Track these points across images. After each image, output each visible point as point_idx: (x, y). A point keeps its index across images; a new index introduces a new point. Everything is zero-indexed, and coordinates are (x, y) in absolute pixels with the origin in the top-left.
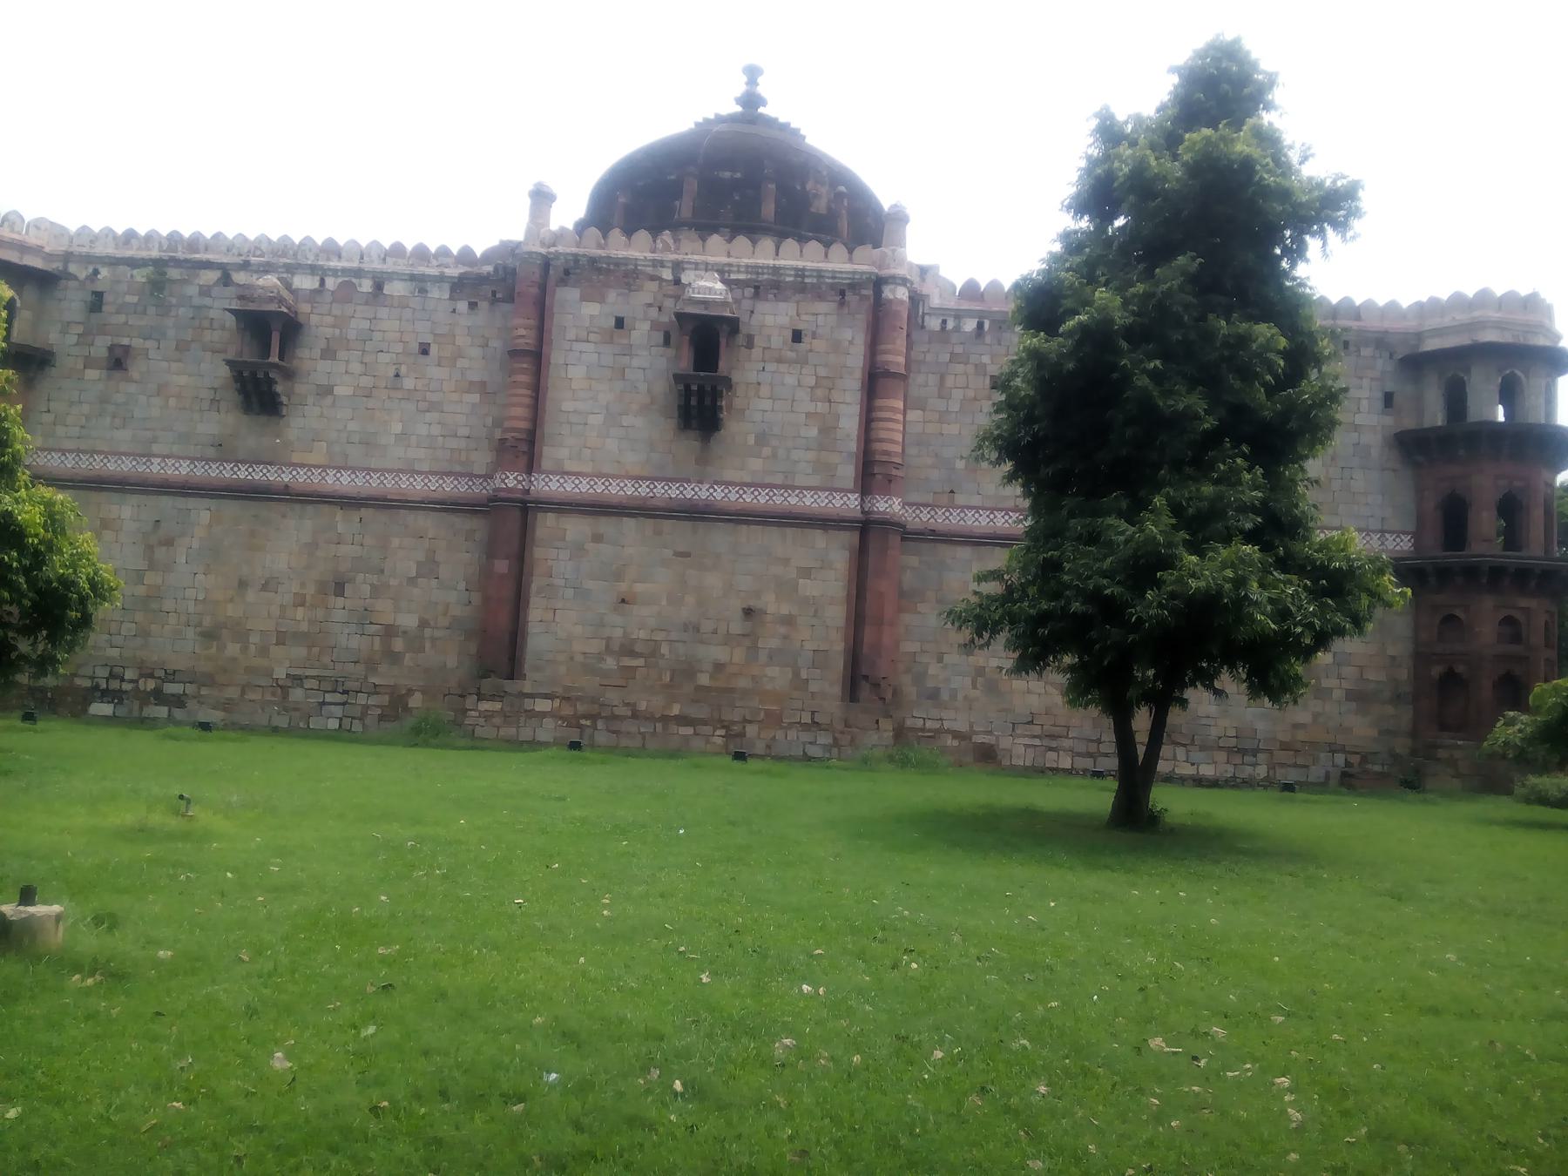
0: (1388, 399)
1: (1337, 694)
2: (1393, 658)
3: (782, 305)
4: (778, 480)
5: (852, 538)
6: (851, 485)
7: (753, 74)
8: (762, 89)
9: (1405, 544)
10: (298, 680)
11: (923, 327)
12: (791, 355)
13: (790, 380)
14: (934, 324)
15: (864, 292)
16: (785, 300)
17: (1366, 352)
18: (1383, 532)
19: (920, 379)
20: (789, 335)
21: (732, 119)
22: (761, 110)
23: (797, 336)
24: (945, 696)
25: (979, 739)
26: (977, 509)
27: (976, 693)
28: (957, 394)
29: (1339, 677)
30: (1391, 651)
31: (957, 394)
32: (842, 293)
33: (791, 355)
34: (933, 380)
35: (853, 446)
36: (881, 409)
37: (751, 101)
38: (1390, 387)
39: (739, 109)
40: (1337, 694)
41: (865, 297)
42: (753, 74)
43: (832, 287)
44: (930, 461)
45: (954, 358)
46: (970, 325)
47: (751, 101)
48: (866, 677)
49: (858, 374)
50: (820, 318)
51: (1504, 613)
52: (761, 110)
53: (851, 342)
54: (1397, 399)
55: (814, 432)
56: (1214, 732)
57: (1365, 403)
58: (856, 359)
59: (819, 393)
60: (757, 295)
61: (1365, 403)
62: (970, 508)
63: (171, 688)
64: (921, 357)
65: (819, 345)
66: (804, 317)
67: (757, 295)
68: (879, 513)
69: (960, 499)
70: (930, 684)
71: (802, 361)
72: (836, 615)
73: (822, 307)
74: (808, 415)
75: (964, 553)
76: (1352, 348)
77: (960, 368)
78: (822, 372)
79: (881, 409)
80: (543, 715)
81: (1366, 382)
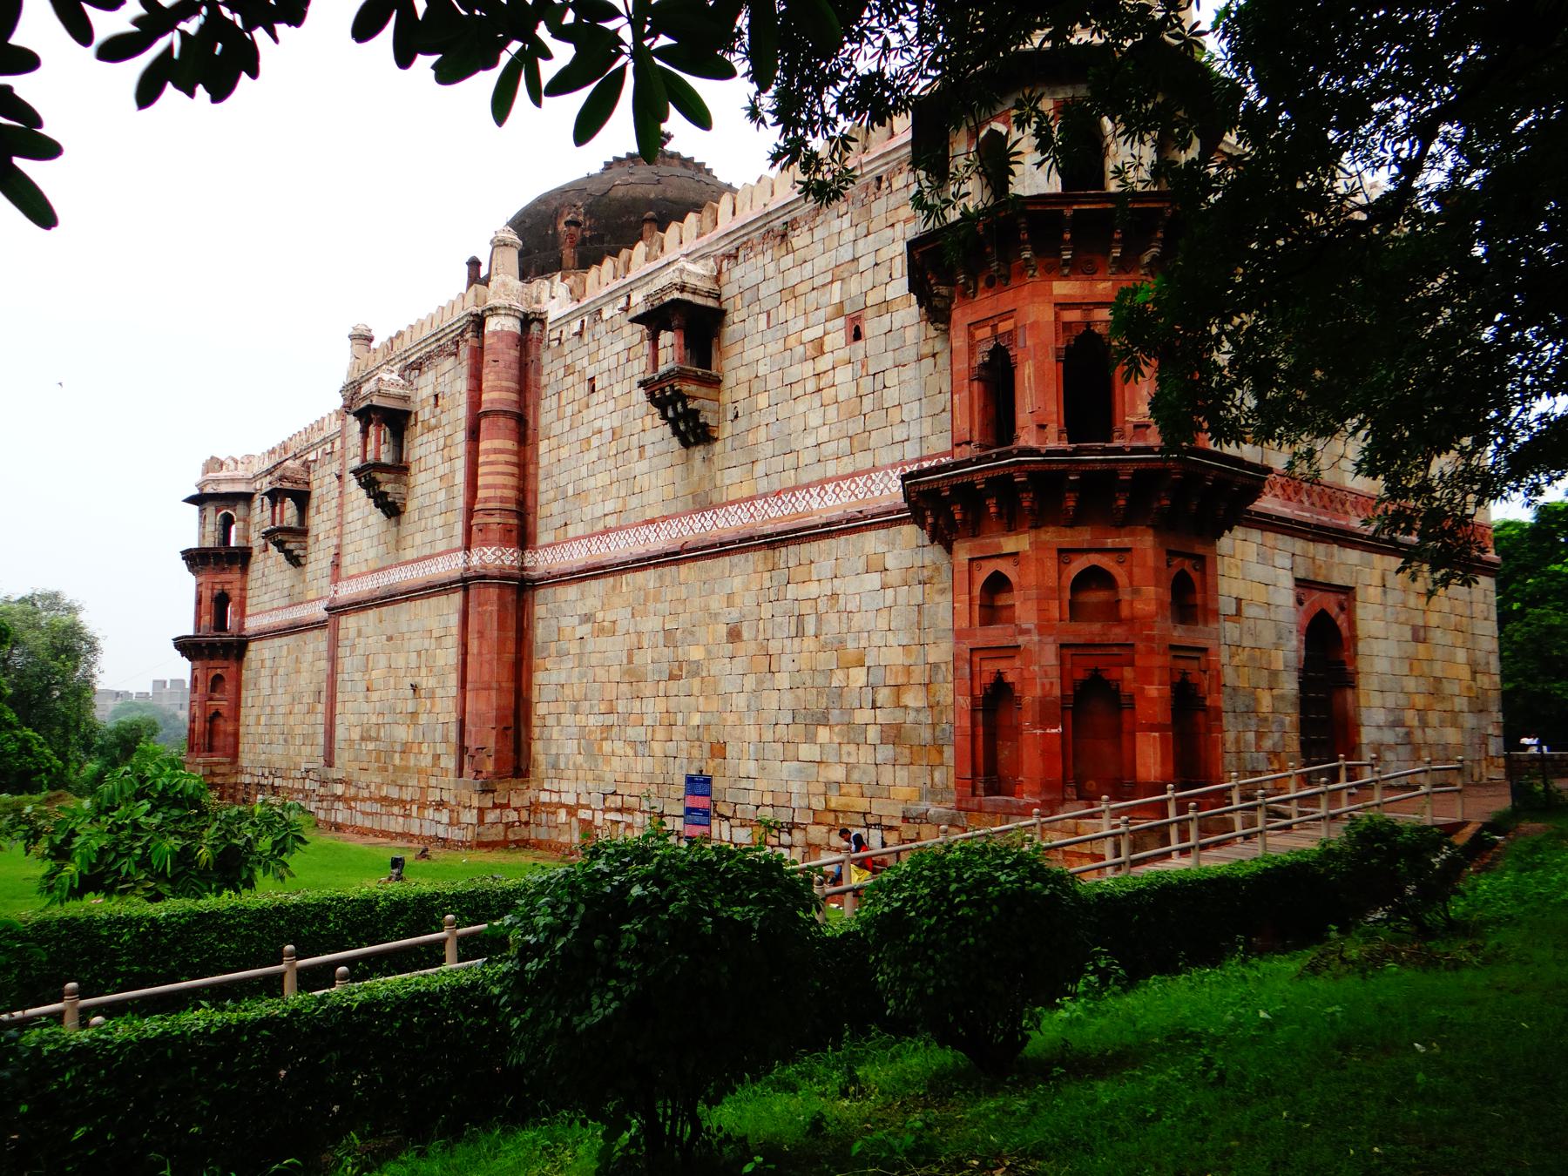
1: (873, 734)
4: (427, 551)
5: (457, 598)
10: (307, 771)
12: (433, 421)
20: (432, 401)
25: (584, 814)
28: (569, 410)
29: (874, 707)
31: (569, 410)
34: (555, 398)
44: (551, 494)
45: (569, 370)
46: (576, 326)
55: (442, 496)
56: (753, 798)
58: (462, 412)
62: (576, 539)
63: (277, 782)
69: (572, 531)
72: (453, 680)
75: (572, 591)
76: (884, 185)
80: (338, 798)
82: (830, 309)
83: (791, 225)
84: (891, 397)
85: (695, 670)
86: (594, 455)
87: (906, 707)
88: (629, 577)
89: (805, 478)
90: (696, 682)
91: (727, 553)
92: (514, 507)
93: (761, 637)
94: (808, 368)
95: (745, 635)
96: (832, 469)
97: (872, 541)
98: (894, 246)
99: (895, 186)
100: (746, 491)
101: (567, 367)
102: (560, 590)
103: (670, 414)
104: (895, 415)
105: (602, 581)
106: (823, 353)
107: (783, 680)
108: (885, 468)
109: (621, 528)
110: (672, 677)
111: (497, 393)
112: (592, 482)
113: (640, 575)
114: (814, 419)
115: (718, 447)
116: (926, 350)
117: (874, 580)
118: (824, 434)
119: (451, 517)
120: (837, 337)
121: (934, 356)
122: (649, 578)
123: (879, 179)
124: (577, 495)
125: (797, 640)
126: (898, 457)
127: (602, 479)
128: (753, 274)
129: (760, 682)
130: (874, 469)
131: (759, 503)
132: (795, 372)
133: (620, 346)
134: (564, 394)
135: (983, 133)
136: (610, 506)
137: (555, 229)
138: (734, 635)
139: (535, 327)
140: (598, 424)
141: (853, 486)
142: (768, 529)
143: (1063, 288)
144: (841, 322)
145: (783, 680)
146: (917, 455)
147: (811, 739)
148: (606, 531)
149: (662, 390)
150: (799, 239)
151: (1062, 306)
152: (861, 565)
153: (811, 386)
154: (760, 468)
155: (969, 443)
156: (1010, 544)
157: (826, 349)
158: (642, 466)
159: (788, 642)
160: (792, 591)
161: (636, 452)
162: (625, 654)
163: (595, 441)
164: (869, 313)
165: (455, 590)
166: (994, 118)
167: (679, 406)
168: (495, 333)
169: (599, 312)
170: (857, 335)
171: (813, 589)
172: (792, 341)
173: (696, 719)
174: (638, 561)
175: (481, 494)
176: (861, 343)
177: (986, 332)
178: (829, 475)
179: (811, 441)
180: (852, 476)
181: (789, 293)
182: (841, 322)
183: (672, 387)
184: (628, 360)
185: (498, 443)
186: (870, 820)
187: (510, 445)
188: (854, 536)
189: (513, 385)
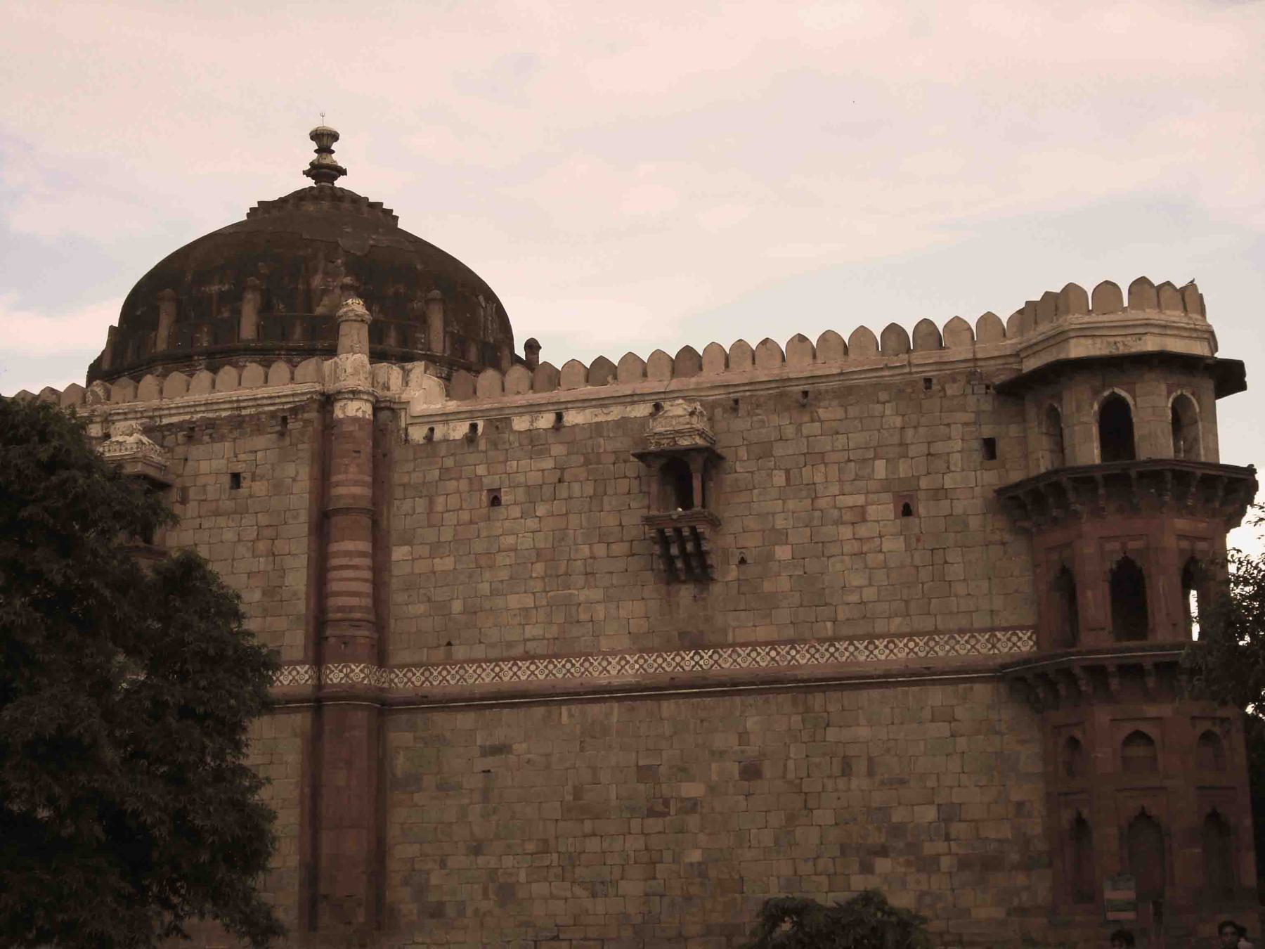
0: (990, 447)
2: (1020, 805)
3: (217, 446)
6: (299, 654)
7: (324, 139)
8: (341, 155)
9: (1025, 644)
11: (406, 441)
12: (228, 505)
13: (229, 536)
14: (417, 434)
15: (306, 416)
16: (222, 438)
17: (951, 390)
18: (992, 630)
19: (406, 506)
20: (226, 480)
21: (299, 197)
22: (340, 183)
23: (236, 479)
24: (450, 911)
26: (478, 661)
27: (485, 905)
28: (451, 518)
29: (948, 838)
30: (1016, 796)
31: (451, 518)
32: (284, 420)
33: (228, 505)
34: (421, 505)
35: (301, 607)
36: (337, 554)
37: (324, 172)
38: (987, 432)
39: (310, 182)
40: (945, 862)
41: (307, 422)
42: (324, 139)
43: (273, 415)
44: (421, 608)
46: (460, 430)
47: (324, 172)
48: (325, 897)
49: (303, 517)
50: (260, 455)
51: (1128, 728)
52: (340, 183)
53: (294, 480)
54: (1001, 447)
57: (956, 458)
59: (262, 546)
60: (190, 439)
61: (956, 458)
62: (473, 661)
64: (406, 480)
65: (260, 488)
66: (242, 457)
67: (190, 439)
68: (334, 685)
69: (459, 652)
70: (432, 898)
71: (241, 511)
73: (261, 441)
74: (250, 575)
75: (465, 720)
76: (935, 387)
77: (452, 485)
78: (263, 520)
79: (337, 554)
81: (956, 431)
82: (873, 485)
83: (819, 396)
84: (956, 570)
85: (692, 806)
86: (504, 574)
87: (987, 838)
88: (575, 709)
89: (846, 631)
90: (693, 821)
91: (739, 693)
92: (371, 617)
93: (791, 776)
94: (846, 532)
95: (768, 770)
96: (880, 626)
97: (936, 696)
98: (951, 443)
99: (949, 392)
100: (762, 633)
101: (444, 470)
102: (439, 718)
103: (674, 550)
104: (960, 589)
105: (522, 712)
106: (864, 520)
107: (825, 816)
108: (950, 632)
109: (557, 656)
110: (652, 813)
111: (351, 485)
112: (499, 602)
113: (595, 710)
114: (857, 580)
115: (716, 589)
116: (997, 537)
117: (943, 729)
118: (870, 594)
119: (281, 624)
120: (883, 510)
121: (1003, 544)
122: (616, 713)
123: (928, 381)
124: (471, 612)
125: (841, 783)
126: (963, 622)
127: (514, 601)
128: (764, 431)
129: (791, 818)
130: (937, 631)
131: (783, 650)
132: (829, 530)
133: (548, 464)
134: (440, 500)
135: (1106, 393)
136: (530, 631)
137: (308, 284)
138: (751, 772)
139: (384, 415)
140: (510, 540)
141: (911, 645)
142: (803, 674)
143: (1181, 524)
144: (887, 497)
145: (825, 816)
146: (988, 625)
147: (867, 869)
148: (530, 657)
149: (678, 531)
150: (829, 412)
151: (1181, 537)
152: (927, 714)
153: (847, 548)
154: (783, 615)
155: (1103, 629)
156: (1152, 711)
157: (868, 518)
158: (597, 594)
159: (830, 784)
160: (832, 734)
161: (581, 580)
162: (569, 788)
163: (502, 559)
164: (921, 495)
165: (297, 710)
166: (1120, 386)
167: (690, 547)
168: (355, 420)
169: (507, 420)
170: (907, 511)
171: (863, 732)
172: (822, 503)
173: (695, 856)
174: (594, 693)
175: (333, 602)
176: (911, 518)
177: (1116, 546)
178: (878, 630)
179: (854, 598)
180: (911, 635)
181: (816, 457)
182: (887, 497)
183: (693, 529)
184: (560, 481)
185: (349, 545)
186: (947, 938)
187: (365, 546)
188: (916, 689)
189: (368, 479)
